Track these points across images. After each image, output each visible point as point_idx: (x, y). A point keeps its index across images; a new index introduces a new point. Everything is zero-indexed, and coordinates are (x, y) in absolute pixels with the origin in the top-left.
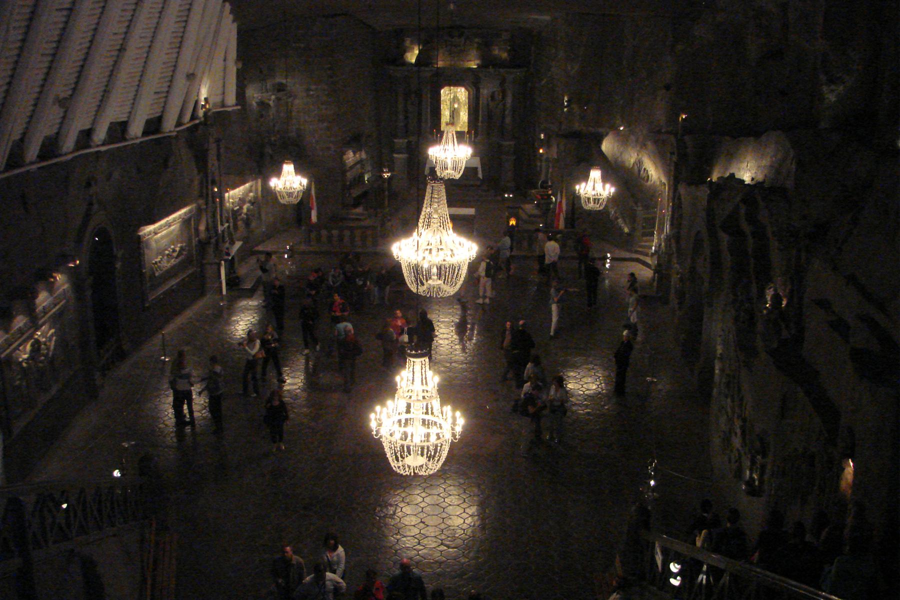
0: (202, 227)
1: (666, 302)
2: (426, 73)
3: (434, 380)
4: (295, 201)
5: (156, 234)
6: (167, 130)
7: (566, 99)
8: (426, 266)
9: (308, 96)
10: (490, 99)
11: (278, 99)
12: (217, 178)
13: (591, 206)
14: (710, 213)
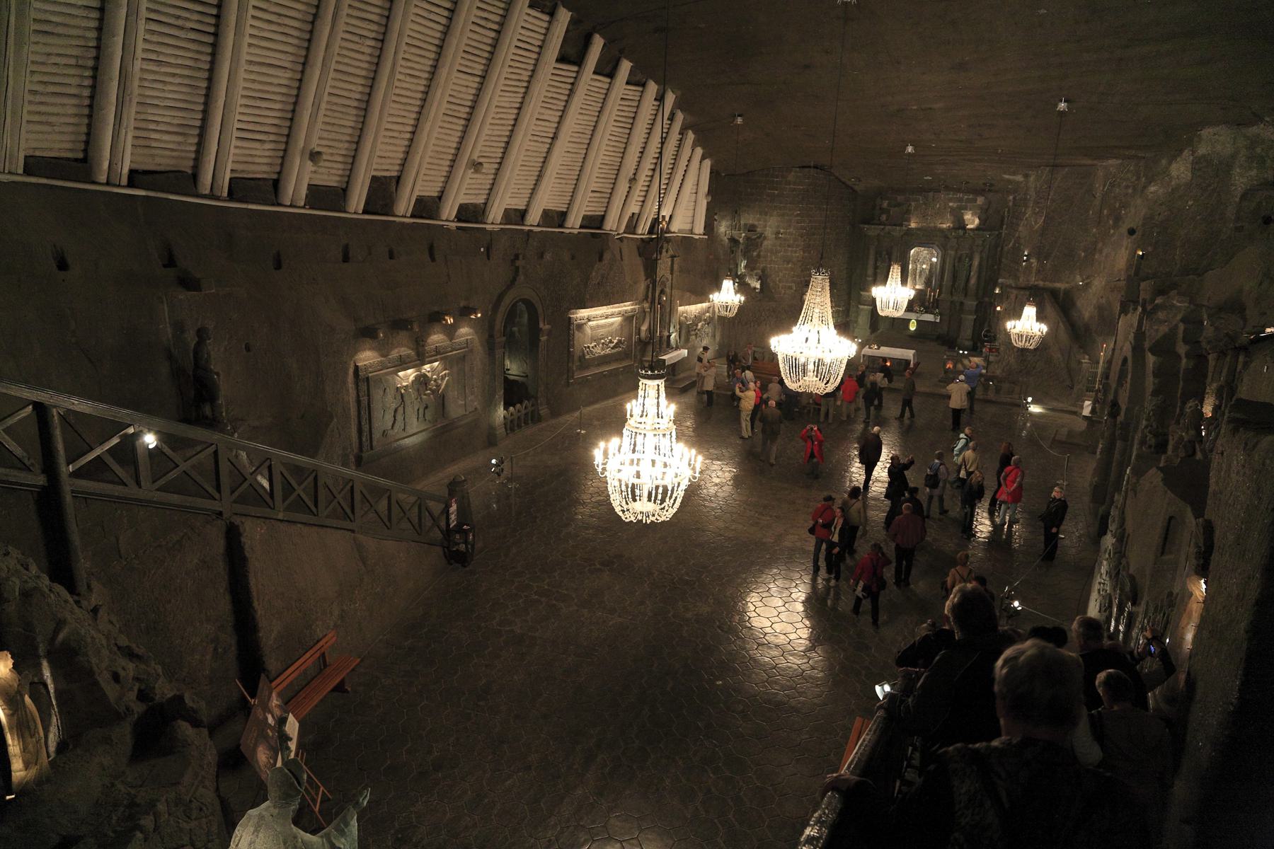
0: (644, 328)
5: (589, 320)
6: (608, 228)
7: (1026, 253)
8: (802, 360)
9: (776, 238)
11: (747, 238)
12: (668, 290)
13: (1020, 345)
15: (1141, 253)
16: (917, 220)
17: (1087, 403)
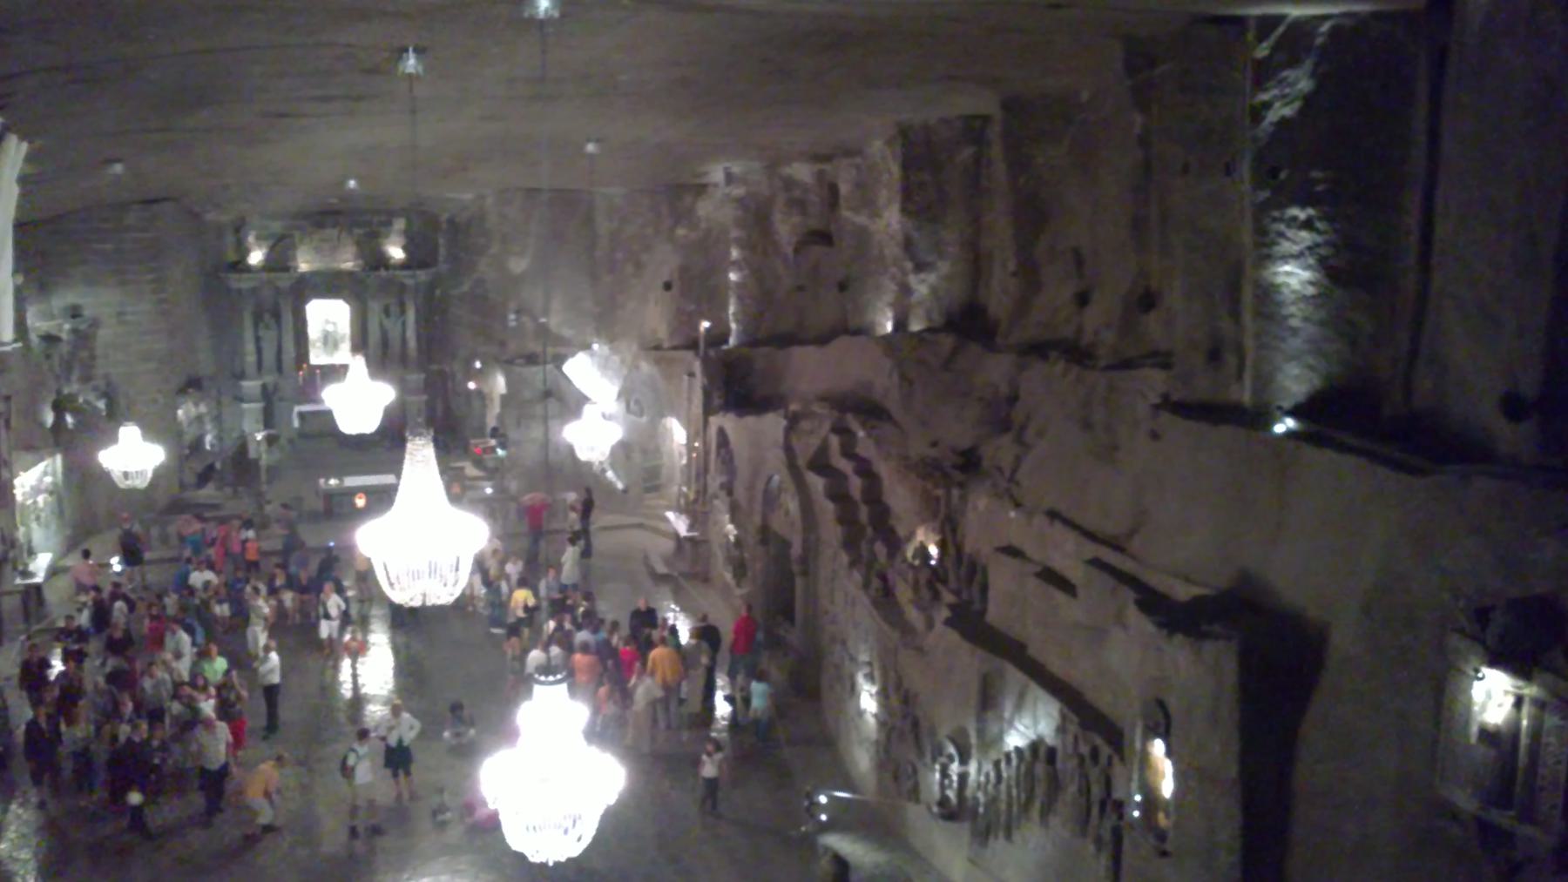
1: (705, 579)
2: (284, 281)
3: (579, 712)
4: (141, 483)
10: (383, 316)
14: (788, 449)
15: (705, 324)
16: (308, 258)
17: (670, 515)
